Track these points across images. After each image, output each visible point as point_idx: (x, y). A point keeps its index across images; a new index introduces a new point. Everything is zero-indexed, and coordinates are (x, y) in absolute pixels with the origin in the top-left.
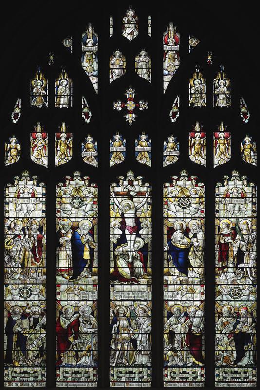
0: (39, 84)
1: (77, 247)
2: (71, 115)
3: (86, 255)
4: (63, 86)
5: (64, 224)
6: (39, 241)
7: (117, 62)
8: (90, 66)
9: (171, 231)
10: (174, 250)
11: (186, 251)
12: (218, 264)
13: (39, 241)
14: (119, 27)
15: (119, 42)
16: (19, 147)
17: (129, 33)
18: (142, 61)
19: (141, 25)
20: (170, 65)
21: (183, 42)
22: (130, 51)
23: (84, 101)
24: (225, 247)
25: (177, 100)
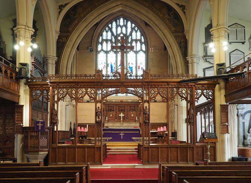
0: (104, 33)
1: (112, 67)
2: (111, 41)
3: (113, 68)
4: (109, 33)
5: (109, 62)
6: (105, 65)
7: (119, 29)
8: (114, 30)
9: (129, 63)
10: (130, 67)
11: (132, 67)
12: (138, 70)
13: (105, 65)
14: (119, 22)
15: (119, 25)
16: (101, 46)
17: (122, 24)
18: (124, 29)
19: (124, 22)
20: (129, 30)
21: (132, 25)
22: (121, 27)
23: (113, 37)
24: (139, 67)
25: (130, 37)
